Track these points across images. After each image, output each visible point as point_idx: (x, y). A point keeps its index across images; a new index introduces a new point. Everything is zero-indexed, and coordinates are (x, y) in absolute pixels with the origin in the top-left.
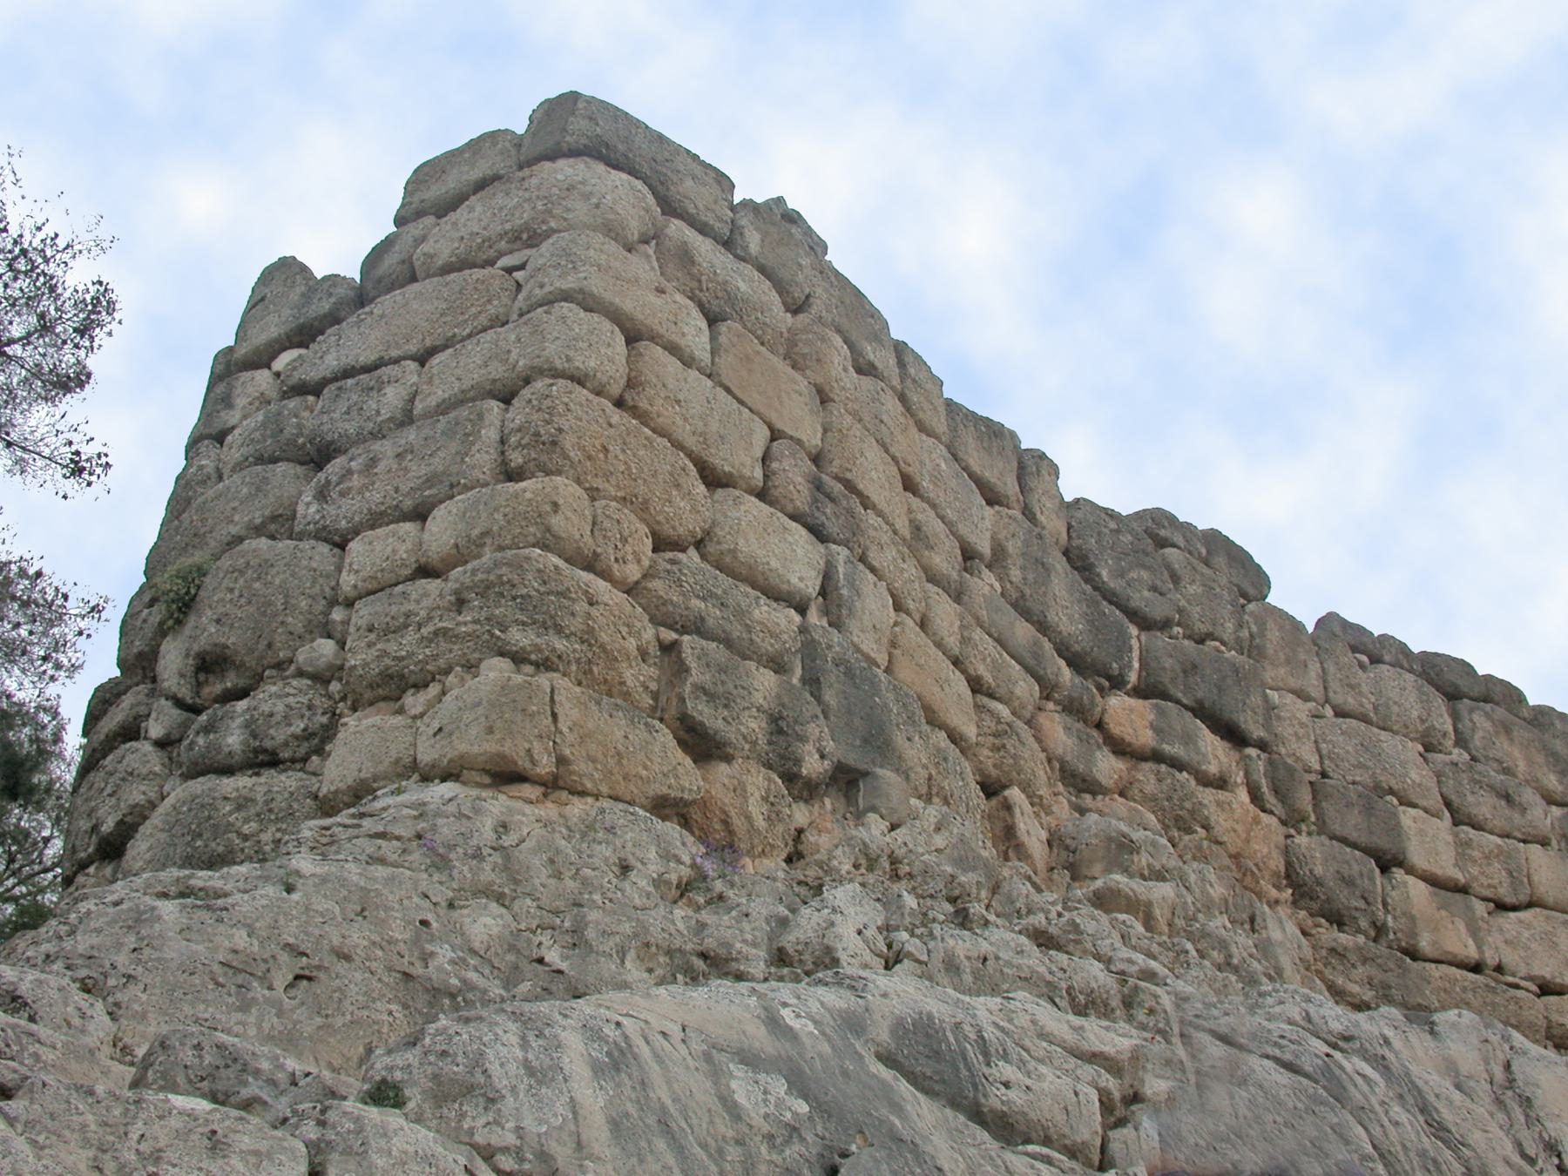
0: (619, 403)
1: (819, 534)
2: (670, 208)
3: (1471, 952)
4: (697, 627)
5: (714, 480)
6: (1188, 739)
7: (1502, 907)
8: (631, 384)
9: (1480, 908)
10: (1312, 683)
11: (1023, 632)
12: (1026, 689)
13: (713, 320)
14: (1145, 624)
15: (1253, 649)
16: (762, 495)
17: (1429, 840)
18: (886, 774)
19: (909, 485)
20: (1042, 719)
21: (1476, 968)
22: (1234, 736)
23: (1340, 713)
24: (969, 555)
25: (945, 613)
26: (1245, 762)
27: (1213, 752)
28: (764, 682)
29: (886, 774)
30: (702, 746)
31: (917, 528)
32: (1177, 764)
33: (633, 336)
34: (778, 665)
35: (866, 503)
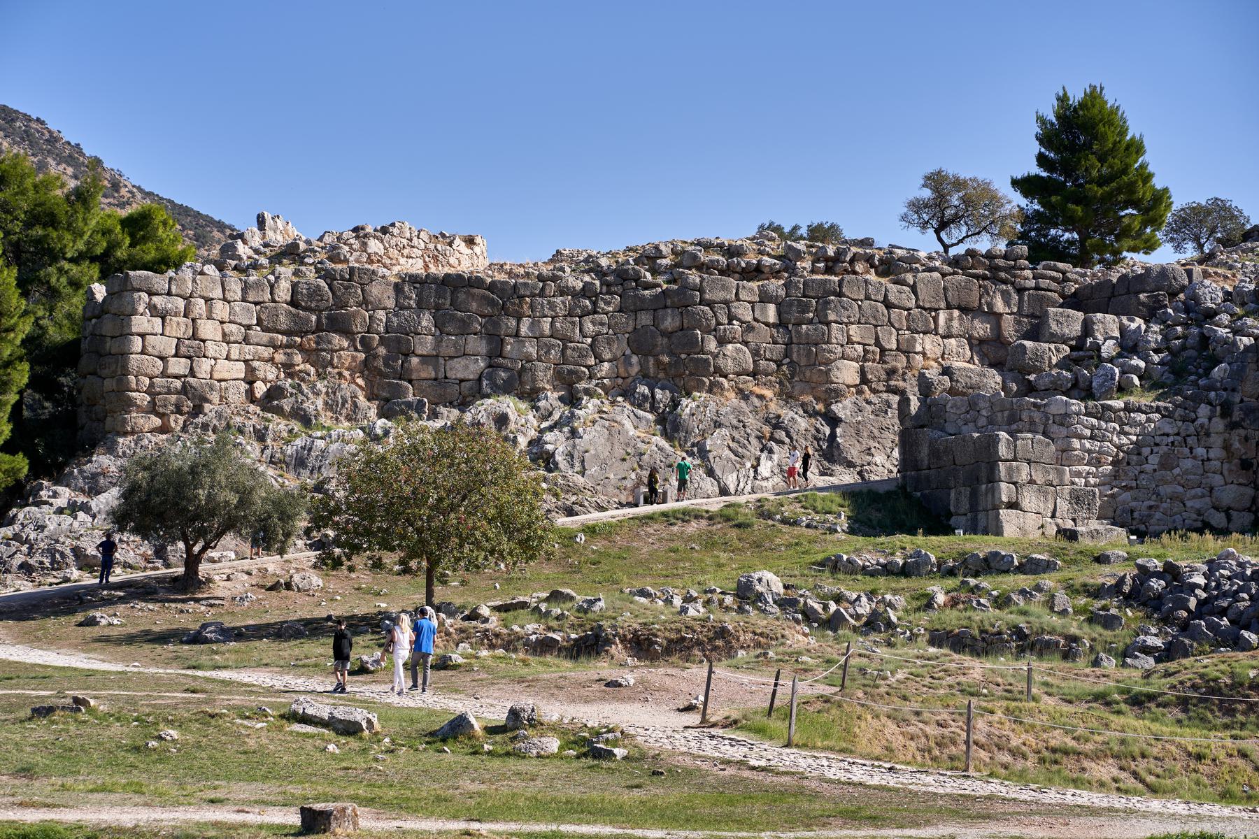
0: (142, 353)
1: (189, 358)
2: (151, 294)
3: (433, 375)
4: (160, 393)
5: (162, 358)
6: (330, 342)
7: (451, 358)
8: (144, 346)
9: (441, 361)
10: (391, 303)
11: (266, 336)
12: (266, 352)
13: (163, 319)
14: (317, 311)
15: (365, 303)
16: (176, 355)
17: (425, 344)
18: (206, 405)
19: (222, 323)
20: (276, 355)
21: (435, 379)
22: (347, 333)
23: (401, 309)
24: (249, 327)
25: (235, 350)
26: (353, 341)
27: (338, 340)
28: (173, 398)
29: (206, 405)
30: (161, 416)
31: (224, 334)
32: (324, 350)
33: (143, 336)
34: (178, 392)
35: (204, 341)
